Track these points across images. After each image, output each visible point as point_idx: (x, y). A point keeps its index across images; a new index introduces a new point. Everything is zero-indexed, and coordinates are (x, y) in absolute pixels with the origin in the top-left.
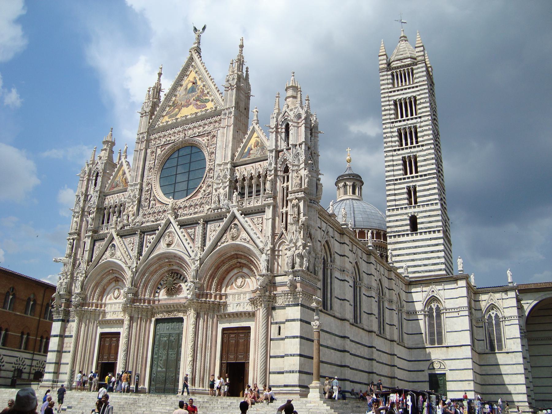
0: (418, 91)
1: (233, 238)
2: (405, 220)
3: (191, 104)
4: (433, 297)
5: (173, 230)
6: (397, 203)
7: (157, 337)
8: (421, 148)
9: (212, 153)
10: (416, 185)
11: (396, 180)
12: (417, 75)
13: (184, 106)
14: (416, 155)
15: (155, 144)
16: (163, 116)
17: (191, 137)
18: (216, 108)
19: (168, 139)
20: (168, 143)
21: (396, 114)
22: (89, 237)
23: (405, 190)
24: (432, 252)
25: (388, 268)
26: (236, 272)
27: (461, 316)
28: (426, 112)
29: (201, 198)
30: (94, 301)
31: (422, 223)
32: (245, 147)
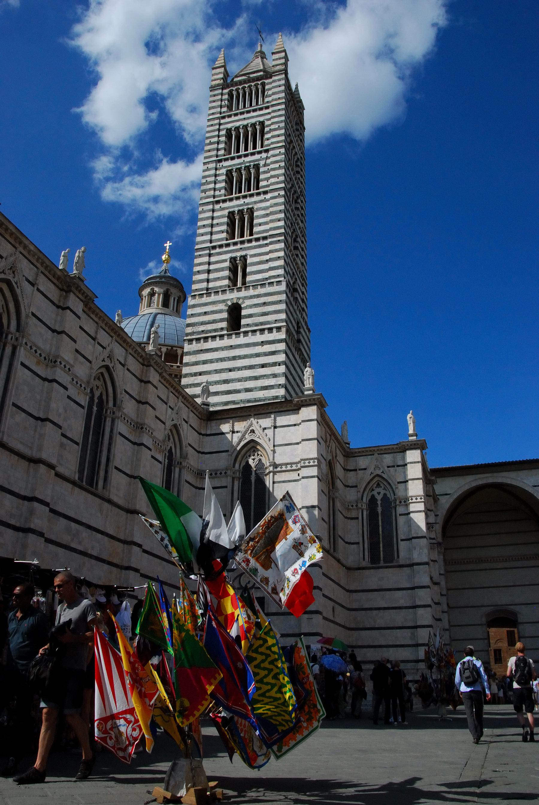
0: (269, 113)
2: (220, 311)
4: (252, 444)
6: (211, 285)
8: (262, 197)
10: (246, 255)
11: (214, 248)
12: (270, 92)
14: (253, 208)
21: (228, 150)
23: (227, 264)
24: (263, 366)
25: (141, 356)
27: (303, 478)
28: (278, 142)
31: (250, 316)
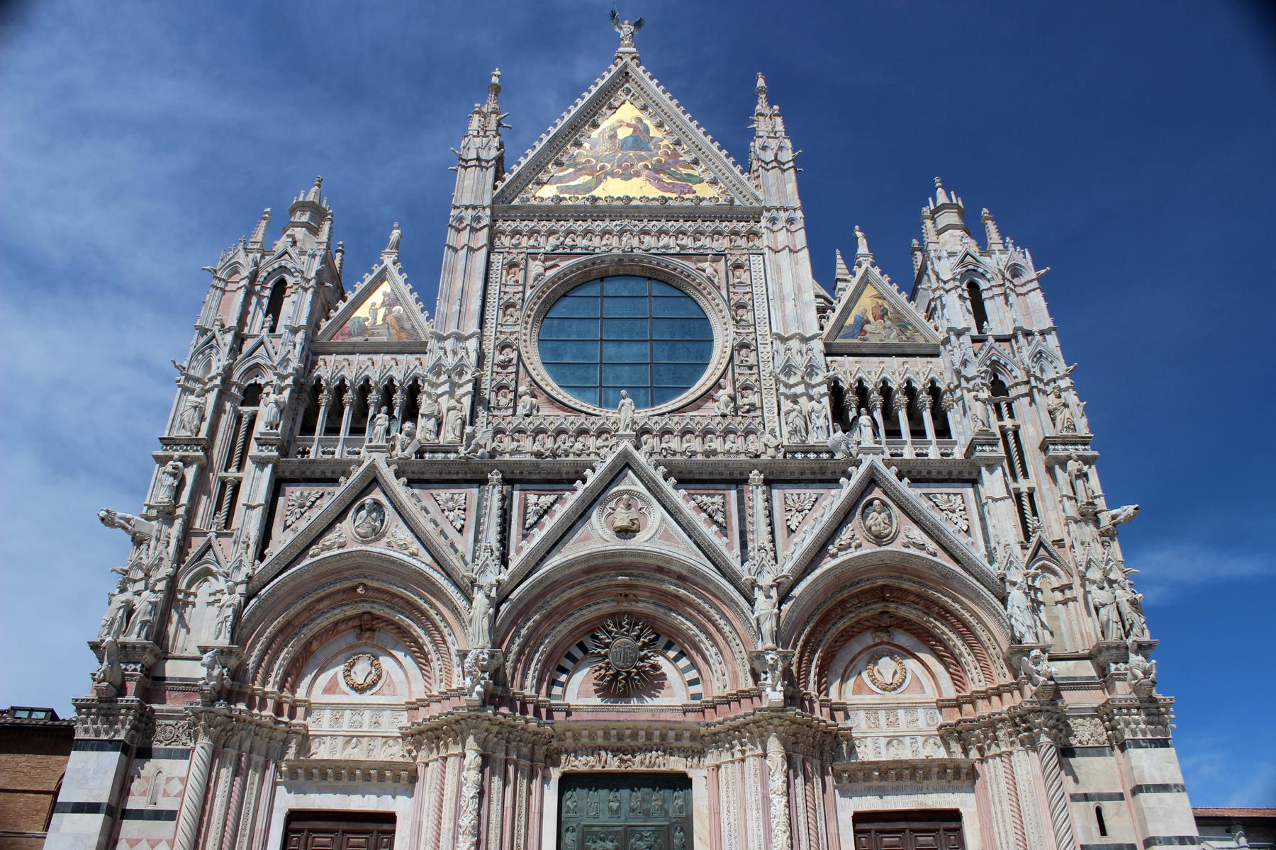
1: (879, 539)
3: (638, 174)
5: (641, 488)
7: (569, 838)
9: (743, 306)
13: (613, 175)
15: (516, 246)
16: (540, 184)
17: (653, 251)
18: (732, 201)
19: (568, 241)
20: (568, 251)
22: (261, 463)
26: (871, 643)
29: (724, 416)
30: (268, 688)
32: (847, 311)
